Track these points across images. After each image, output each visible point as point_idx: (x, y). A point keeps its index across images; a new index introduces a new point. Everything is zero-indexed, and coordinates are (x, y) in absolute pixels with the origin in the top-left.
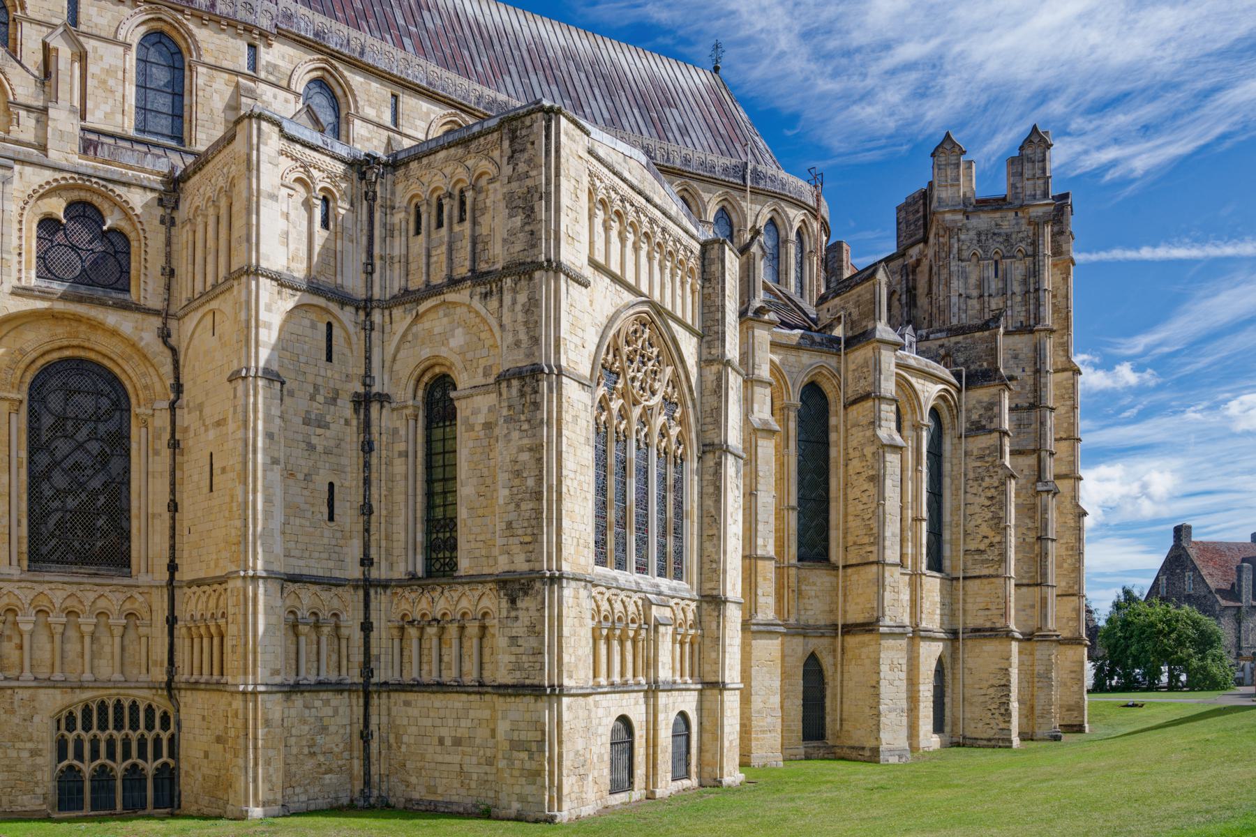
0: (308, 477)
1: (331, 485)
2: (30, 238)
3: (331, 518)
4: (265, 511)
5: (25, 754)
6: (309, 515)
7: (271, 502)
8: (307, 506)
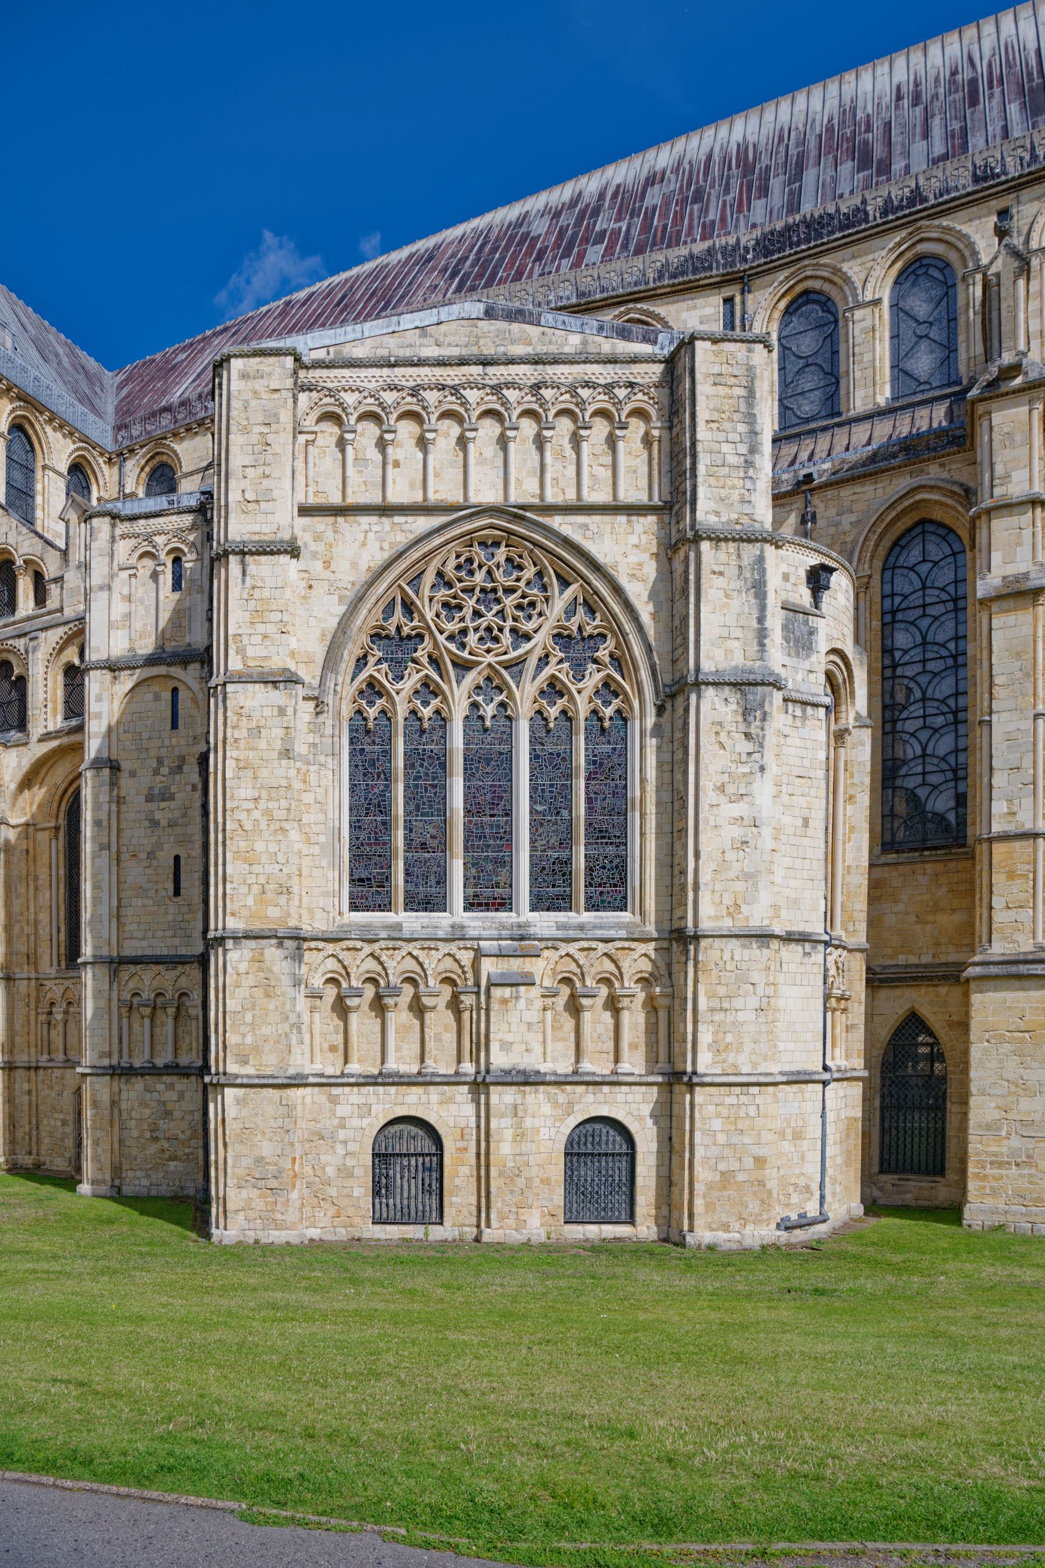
0: (151, 855)
1: (177, 858)
2: (55, 690)
3: (177, 892)
4: (94, 898)
5: (59, 1123)
6: (152, 893)
7: (99, 887)
8: (150, 885)
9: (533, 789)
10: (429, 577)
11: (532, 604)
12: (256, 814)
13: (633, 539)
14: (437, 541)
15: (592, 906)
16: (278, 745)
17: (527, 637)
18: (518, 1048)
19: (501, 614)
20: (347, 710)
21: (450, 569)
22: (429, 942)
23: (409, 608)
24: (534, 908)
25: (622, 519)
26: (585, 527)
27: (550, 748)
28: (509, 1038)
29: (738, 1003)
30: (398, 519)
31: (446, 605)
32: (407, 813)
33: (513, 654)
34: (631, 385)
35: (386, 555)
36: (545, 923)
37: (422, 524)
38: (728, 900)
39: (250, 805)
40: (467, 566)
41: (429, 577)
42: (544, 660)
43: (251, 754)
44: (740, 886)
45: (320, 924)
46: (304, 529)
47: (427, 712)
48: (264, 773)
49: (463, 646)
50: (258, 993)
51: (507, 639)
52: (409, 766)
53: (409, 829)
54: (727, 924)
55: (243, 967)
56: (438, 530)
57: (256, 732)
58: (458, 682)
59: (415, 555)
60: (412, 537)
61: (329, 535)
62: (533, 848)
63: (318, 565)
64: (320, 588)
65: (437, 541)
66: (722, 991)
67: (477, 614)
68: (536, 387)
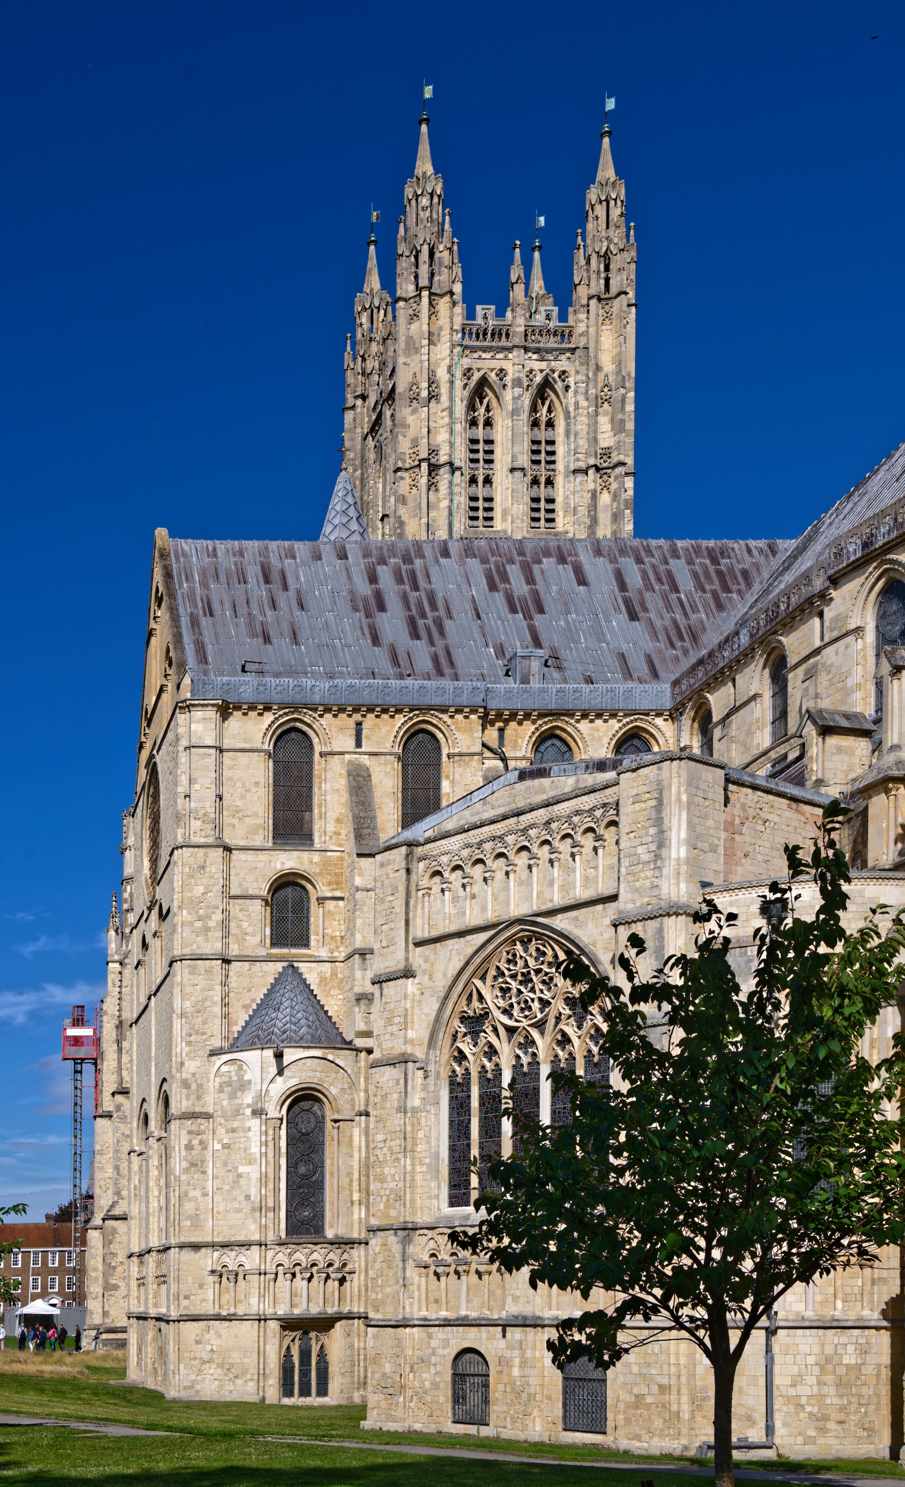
10: (493, 972)
11: (551, 979)
12: (385, 1150)
14: (490, 948)
16: (396, 1104)
18: (522, 1300)
19: (533, 990)
20: (445, 1074)
21: (503, 966)
25: (599, 907)
28: (518, 1293)
30: (469, 938)
31: (501, 989)
32: (481, 1137)
33: (539, 1016)
34: (604, 805)
35: (462, 964)
37: (483, 937)
39: (381, 1145)
40: (512, 961)
42: (558, 1019)
43: (382, 1112)
46: (418, 957)
47: (488, 1065)
48: (388, 1123)
49: (511, 1016)
50: (385, 1265)
51: (536, 1006)
52: (482, 1104)
55: (377, 1249)
56: (489, 941)
57: (385, 1097)
58: (542, 1033)
59: (478, 960)
60: (475, 948)
61: (432, 957)
63: (426, 978)
64: (427, 993)
65: (490, 948)
67: (533, 990)
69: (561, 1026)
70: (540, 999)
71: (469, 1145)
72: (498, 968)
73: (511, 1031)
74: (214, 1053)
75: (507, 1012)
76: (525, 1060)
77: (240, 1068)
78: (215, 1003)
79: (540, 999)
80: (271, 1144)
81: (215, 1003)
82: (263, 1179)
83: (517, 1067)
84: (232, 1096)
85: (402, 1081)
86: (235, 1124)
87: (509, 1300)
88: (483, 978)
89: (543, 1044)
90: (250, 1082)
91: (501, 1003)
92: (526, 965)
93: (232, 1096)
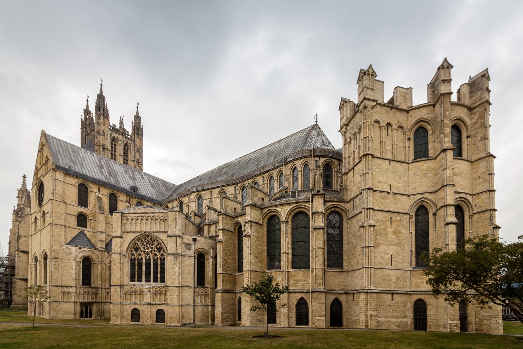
9: (154, 267)
10: (140, 241)
11: (153, 244)
13: (165, 236)
15: (161, 282)
17: (153, 248)
22: (139, 287)
23: (138, 245)
24: (154, 282)
26: (159, 234)
27: (156, 262)
29: (173, 295)
32: (138, 270)
33: (151, 250)
36: (154, 284)
38: (172, 282)
41: (140, 241)
42: (155, 251)
44: (173, 280)
45: (125, 284)
49: (144, 249)
51: (150, 248)
52: (138, 264)
53: (138, 272)
54: (172, 285)
62: (154, 274)
66: (171, 293)
68: (153, 216)
69: (155, 252)
70: (151, 247)
71: (135, 271)
72: (142, 240)
73: (144, 252)
74: (62, 246)
75: (144, 248)
76: (148, 257)
77: (70, 250)
78: (62, 235)
79: (151, 247)
80: (78, 266)
81: (62, 235)
82: (76, 274)
83: (146, 258)
84: (67, 255)
85: (120, 257)
86: (68, 261)
87: (145, 300)
88: (138, 241)
89: (151, 255)
90: (72, 253)
91: (142, 246)
92: (148, 240)
93: (67, 255)
